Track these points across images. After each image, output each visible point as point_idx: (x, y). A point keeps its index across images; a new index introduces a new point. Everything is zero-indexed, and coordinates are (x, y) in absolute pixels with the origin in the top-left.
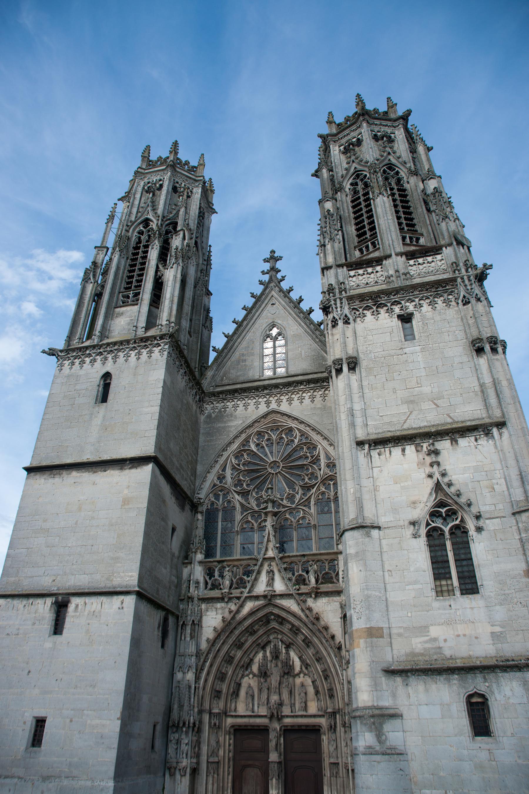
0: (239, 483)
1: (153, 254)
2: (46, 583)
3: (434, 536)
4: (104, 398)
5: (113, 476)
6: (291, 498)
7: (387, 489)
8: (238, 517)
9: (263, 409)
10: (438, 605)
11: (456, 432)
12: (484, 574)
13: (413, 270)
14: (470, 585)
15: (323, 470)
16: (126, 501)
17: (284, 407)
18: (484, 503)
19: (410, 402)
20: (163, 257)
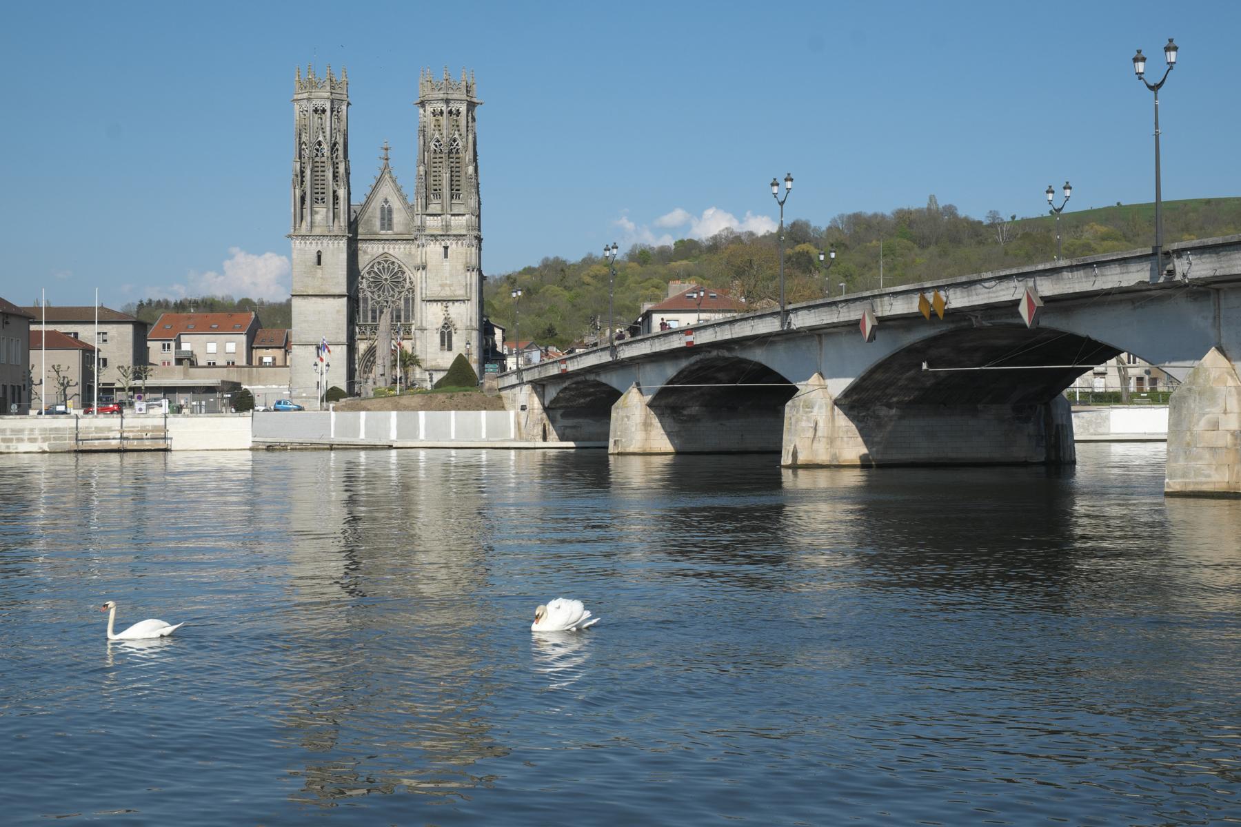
0: (369, 287)
1: (330, 175)
2: (311, 340)
3: (442, 334)
4: (319, 263)
5: (331, 300)
6: (393, 296)
7: (430, 317)
8: (370, 303)
9: (381, 251)
10: (440, 353)
11: (454, 301)
12: (454, 346)
13: (453, 223)
14: (450, 349)
15: (408, 285)
16: (338, 312)
17: (391, 252)
18: (457, 326)
19: (442, 286)
20: (335, 177)
